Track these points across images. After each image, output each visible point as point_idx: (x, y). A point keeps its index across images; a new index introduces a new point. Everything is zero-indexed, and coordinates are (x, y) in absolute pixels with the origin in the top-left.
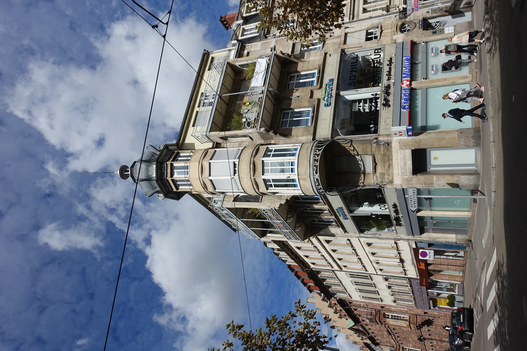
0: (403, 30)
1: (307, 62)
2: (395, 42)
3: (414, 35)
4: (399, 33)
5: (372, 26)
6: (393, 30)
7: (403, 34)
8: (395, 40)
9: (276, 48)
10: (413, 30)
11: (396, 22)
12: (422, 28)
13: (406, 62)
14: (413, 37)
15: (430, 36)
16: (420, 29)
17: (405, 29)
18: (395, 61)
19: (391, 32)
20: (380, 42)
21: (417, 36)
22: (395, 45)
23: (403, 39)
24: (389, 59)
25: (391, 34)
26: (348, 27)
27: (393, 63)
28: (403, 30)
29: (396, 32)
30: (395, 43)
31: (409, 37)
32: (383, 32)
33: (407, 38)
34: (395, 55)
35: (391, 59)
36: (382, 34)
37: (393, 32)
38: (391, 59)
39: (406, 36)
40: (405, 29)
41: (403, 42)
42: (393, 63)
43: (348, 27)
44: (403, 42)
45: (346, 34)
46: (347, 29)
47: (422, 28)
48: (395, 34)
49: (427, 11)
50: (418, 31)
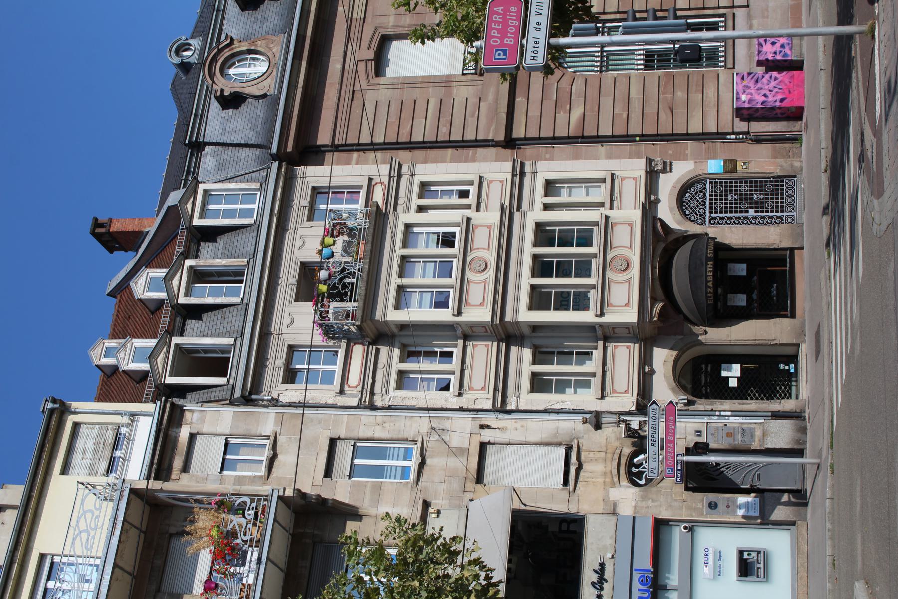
0: (634, 470)
1: (372, 520)
2: (614, 509)
3: (662, 498)
4: (625, 482)
5: (554, 440)
6: (609, 469)
7: (635, 490)
8: (615, 505)
9: (279, 444)
10: (660, 484)
11: (617, 444)
12: (681, 482)
13: (641, 587)
14: (660, 506)
15: (702, 514)
16: (677, 482)
17: (640, 469)
18: (611, 574)
19: (605, 473)
20: (574, 498)
21: (670, 506)
22: (614, 518)
23: (635, 507)
24: (597, 567)
25: (604, 482)
26: (488, 427)
27: (606, 581)
28: (634, 470)
29: (616, 479)
30: (614, 513)
31: (650, 502)
32: (585, 466)
33: (644, 504)
34: (613, 556)
35: (602, 565)
36: (582, 474)
37: (609, 475)
38: (602, 565)
39: (644, 498)
40: (640, 469)
41: (634, 518)
42: (606, 581)
43: (488, 427)
44: (634, 518)
45: (483, 446)
46: (486, 430)
47: (681, 482)
48: (613, 485)
49: (697, 427)
50: (671, 489)
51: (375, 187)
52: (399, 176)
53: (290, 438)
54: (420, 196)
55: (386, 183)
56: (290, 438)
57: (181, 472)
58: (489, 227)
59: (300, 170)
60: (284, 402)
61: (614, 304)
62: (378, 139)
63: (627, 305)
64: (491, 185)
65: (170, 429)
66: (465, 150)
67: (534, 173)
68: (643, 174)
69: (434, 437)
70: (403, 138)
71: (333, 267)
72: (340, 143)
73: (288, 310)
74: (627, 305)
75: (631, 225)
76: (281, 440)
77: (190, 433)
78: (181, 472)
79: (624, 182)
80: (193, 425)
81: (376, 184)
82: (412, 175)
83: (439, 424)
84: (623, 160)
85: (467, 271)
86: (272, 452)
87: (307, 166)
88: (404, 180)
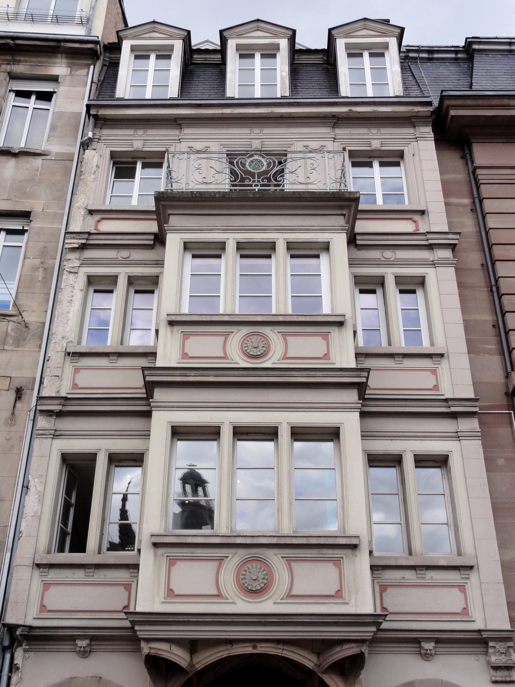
9: (31, 159)
51: (410, 222)
52: (430, 247)
53: (37, 170)
54: (399, 280)
55: (418, 232)
56: (37, 170)
57: (9, 73)
58: (326, 356)
59: (428, 131)
60: (85, 156)
61: (173, 569)
62: (492, 222)
63: (170, 593)
64: (429, 373)
65: (63, 55)
66: (493, 339)
67: (457, 436)
68: (478, 625)
69: (12, 330)
70: (498, 252)
71: (252, 161)
72: (480, 177)
73: (214, 146)
74: (170, 593)
75: (339, 594)
76: (38, 162)
77: (58, 76)
78: (9, 73)
79: (456, 591)
80: (69, 78)
81: (415, 222)
82: (433, 264)
83: (33, 335)
84: (502, 586)
85: (245, 330)
86: (17, 151)
87: (435, 140)
88: (424, 254)
